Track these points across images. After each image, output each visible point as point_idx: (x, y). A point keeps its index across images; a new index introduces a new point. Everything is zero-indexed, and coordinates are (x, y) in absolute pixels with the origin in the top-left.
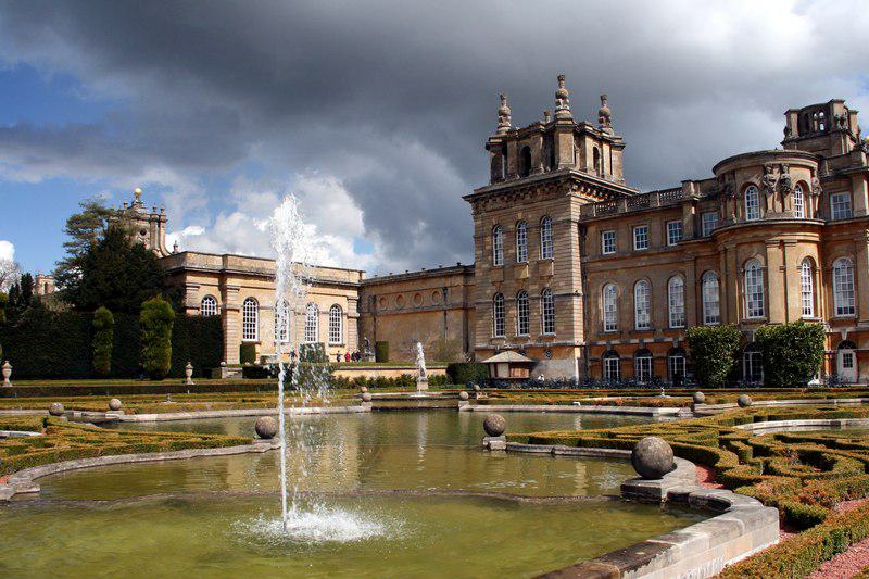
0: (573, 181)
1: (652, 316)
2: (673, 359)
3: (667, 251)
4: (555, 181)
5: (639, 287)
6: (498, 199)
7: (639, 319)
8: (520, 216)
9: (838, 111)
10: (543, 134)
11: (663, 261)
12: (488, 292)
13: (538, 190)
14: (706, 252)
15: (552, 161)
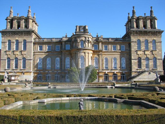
0: (33, 32)
1: (51, 66)
2: (56, 76)
3: (56, 52)
4: (29, 31)
5: (48, 59)
6: (10, 33)
7: (47, 67)
8: (17, 38)
9: (87, 28)
10: (24, 19)
11: (55, 54)
12: (5, 57)
13: (23, 33)
14: (67, 53)
15: (27, 26)
